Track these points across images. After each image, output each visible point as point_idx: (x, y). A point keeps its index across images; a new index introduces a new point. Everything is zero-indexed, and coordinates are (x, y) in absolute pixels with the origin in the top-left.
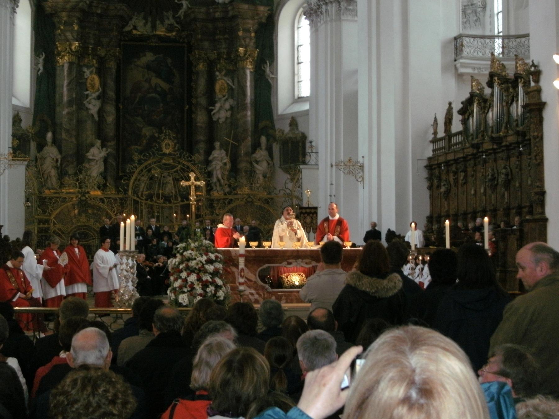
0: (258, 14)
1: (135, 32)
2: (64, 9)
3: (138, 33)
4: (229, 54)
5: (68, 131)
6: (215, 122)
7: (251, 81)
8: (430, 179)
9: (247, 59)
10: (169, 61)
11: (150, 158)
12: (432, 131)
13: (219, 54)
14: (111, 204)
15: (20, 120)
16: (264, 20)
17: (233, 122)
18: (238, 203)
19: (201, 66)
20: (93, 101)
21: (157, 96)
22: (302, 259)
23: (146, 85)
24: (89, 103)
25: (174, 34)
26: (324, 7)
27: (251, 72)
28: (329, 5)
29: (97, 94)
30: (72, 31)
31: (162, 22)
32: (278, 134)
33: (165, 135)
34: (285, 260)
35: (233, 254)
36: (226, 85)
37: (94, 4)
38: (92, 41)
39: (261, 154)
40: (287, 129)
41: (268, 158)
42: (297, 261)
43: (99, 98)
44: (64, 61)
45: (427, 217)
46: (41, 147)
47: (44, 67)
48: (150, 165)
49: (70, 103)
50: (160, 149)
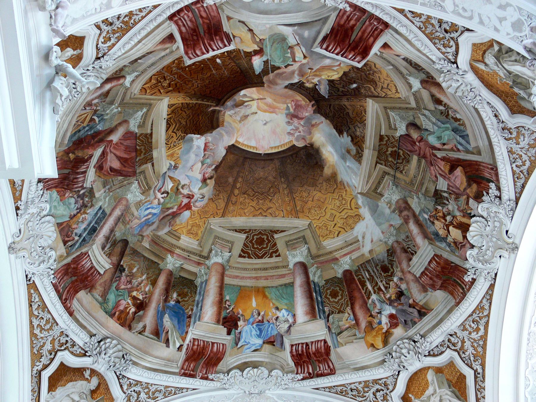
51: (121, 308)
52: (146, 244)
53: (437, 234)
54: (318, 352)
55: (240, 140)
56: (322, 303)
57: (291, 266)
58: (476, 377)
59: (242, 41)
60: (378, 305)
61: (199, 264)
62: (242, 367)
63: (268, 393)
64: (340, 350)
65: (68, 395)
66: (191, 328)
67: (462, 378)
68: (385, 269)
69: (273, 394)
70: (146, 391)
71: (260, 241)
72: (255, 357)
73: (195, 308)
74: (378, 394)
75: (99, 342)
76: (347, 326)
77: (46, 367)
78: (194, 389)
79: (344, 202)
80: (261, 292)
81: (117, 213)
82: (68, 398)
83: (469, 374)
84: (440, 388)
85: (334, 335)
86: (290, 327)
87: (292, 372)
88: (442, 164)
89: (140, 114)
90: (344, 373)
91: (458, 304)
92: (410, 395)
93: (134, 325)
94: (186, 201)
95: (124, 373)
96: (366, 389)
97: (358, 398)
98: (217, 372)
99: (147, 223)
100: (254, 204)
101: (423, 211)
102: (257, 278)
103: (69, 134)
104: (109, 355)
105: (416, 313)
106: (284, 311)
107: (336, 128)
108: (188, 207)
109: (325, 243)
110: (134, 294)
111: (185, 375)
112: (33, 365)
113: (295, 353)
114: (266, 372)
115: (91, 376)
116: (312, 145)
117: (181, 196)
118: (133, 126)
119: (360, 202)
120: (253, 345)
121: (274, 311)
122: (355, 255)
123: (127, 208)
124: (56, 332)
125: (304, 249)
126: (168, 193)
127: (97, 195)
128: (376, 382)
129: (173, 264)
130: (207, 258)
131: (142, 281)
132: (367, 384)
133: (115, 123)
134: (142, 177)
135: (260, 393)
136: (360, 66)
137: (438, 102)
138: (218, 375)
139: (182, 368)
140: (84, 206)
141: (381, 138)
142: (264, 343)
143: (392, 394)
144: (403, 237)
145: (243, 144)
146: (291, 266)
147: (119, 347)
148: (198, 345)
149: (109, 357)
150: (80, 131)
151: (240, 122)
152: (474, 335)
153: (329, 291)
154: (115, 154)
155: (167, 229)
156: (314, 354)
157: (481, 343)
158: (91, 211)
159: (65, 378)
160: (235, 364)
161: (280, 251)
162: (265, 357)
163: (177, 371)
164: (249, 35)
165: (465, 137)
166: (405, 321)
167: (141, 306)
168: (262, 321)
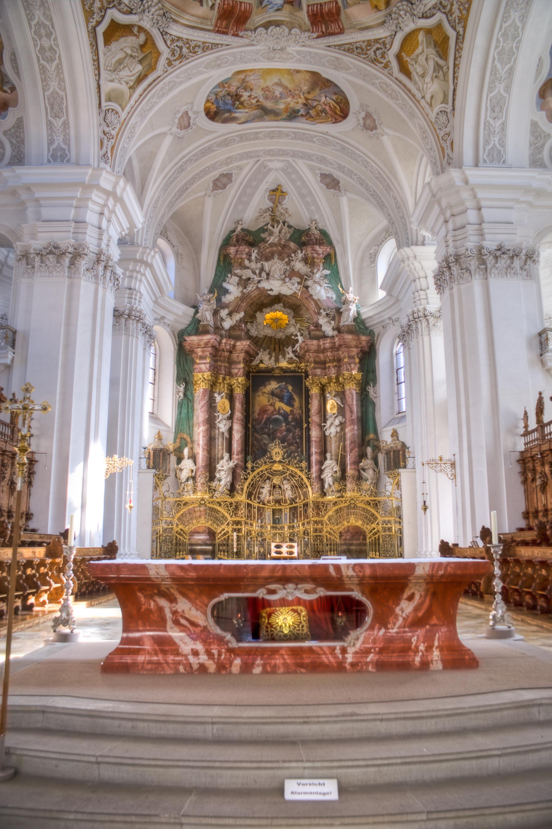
1: (261, 365)
7: (357, 401)
8: (524, 473)
10: (290, 388)
12: (522, 424)
13: (330, 379)
14: (227, 507)
18: (342, 505)
21: (280, 417)
22: (297, 584)
23: (271, 409)
25: (294, 365)
27: (357, 393)
31: (284, 357)
32: (382, 445)
33: (276, 445)
34: (263, 586)
36: (335, 404)
38: (223, 372)
39: (367, 463)
41: (373, 466)
42: (286, 586)
48: (262, 471)
50: (271, 458)
54: (330, 12)
58: (457, 39)
62: (267, 25)
63: (289, 50)
65: (122, 49)
67: (446, 39)
69: (293, 51)
70: (187, 46)
72: (277, 16)
74: (378, 52)
77: (99, 23)
78: (227, 45)
82: (121, 52)
83: (452, 34)
84: (427, 48)
87: (308, 31)
90: (352, 33)
92: (403, 54)
95: (166, 30)
96: (369, 48)
97: (361, 56)
98: (246, 30)
104: (151, 13)
111: (219, 32)
112: (88, 22)
113: (310, 13)
114: (287, 30)
115: (138, 32)
120: (276, 5)
128: (376, 41)
132: (369, 43)
135: (282, 50)
138: (247, 33)
139: (216, 26)
143: (389, 52)
147: (160, 5)
148: (228, 4)
149: (153, 15)
156: (327, 14)
157: (467, 6)
159: (117, 34)
160: (261, 23)
162: (286, 17)
163: (212, 28)
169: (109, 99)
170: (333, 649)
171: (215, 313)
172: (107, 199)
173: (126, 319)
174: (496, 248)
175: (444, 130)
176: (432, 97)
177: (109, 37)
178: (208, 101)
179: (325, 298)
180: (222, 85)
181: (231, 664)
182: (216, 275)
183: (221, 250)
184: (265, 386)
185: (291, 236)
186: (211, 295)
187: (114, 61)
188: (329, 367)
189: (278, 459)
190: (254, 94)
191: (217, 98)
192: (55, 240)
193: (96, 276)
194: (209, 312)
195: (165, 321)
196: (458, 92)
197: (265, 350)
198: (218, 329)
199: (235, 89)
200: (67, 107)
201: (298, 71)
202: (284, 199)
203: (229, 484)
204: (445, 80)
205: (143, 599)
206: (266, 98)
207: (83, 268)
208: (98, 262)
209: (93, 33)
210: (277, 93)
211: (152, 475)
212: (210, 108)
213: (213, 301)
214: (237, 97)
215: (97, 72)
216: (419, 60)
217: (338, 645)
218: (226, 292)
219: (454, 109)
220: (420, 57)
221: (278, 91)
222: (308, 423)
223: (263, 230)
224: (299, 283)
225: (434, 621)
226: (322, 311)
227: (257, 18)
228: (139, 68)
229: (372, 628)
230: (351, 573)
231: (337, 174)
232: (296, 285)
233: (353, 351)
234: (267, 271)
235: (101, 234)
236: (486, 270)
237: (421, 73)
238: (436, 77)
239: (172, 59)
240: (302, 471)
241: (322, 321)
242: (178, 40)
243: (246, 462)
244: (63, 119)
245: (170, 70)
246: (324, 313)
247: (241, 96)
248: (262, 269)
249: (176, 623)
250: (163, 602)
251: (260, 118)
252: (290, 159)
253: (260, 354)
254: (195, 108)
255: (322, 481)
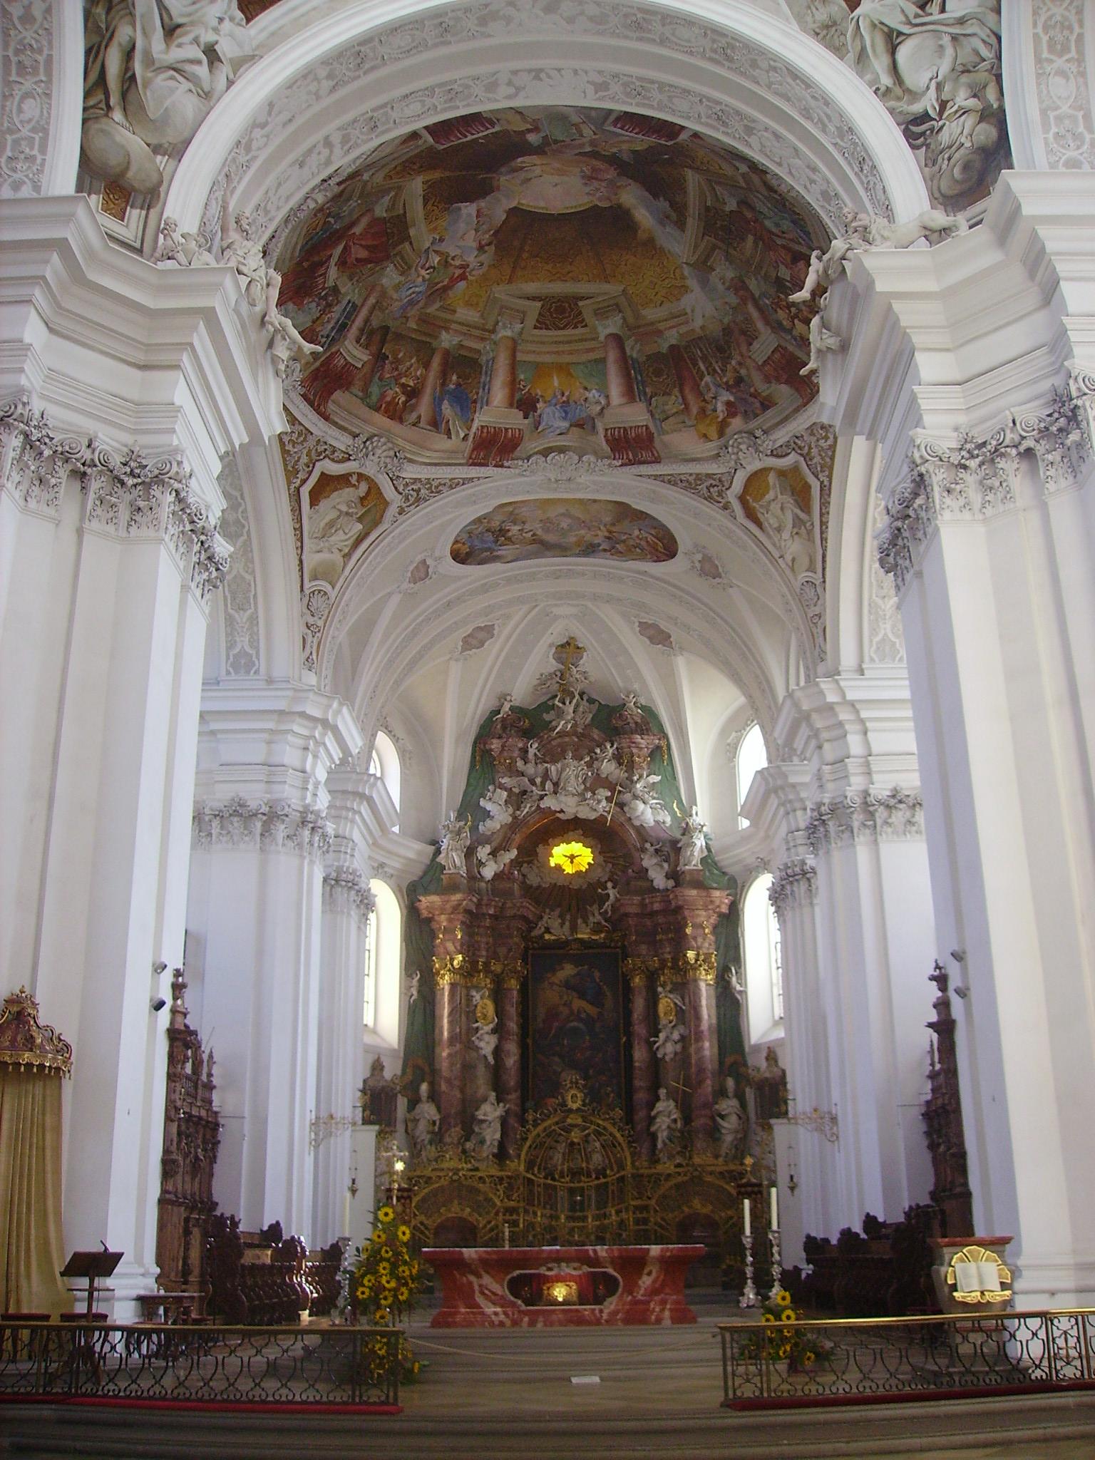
0: (712, 902)
1: (547, 937)
2: (442, 912)
3: (553, 938)
4: (675, 960)
5: (449, 1081)
6: (661, 1059)
8: (928, 1134)
9: (700, 966)
10: (597, 974)
11: (549, 1117)
13: (663, 963)
15: (382, 1068)
16: (724, 909)
17: (683, 1057)
19: (637, 980)
20: (487, 1037)
21: (581, 1025)
24: (480, 1039)
25: (602, 935)
26: (788, 887)
28: (796, 884)
29: (491, 1026)
30: (454, 941)
31: (586, 922)
34: (541, 1265)
35: (466, 1256)
36: (672, 1005)
37: (484, 902)
38: (484, 953)
39: (728, 1105)
40: (763, 1064)
43: (494, 1031)
44: (445, 981)
45: (931, 1193)
46: (414, 1103)
47: (419, 992)
49: (453, 1040)
50: (564, 1104)
51: (388, 399)
52: (412, 325)
53: (780, 324)
55: (523, 202)
56: (643, 383)
57: (602, 338)
59: (508, 122)
60: (713, 389)
61: (483, 339)
62: (545, 453)
64: (666, 438)
66: (477, 414)
67: (807, 487)
68: (720, 349)
71: (561, 310)
72: (559, 441)
73: (481, 391)
74: (712, 490)
75: (365, 443)
76: (675, 410)
77: (304, 482)
79: (666, 270)
80: (564, 369)
81: (372, 300)
84: (782, 494)
85: (658, 422)
86: (603, 409)
87: (608, 458)
88: (783, 252)
89: (387, 198)
91: (805, 405)
93: (406, 416)
94: (458, 272)
98: (512, 459)
99: (412, 303)
100: (549, 267)
101: (764, 295)
102: (557, 353)
103: (299, 247)
105: (758, 405)
106: (594, 391)
107: (649, 190)
108: (463, 277)
109: (644, 312)
110: (403, 380)
112: (289, 483)
114: (576, 458)
116: (620, 206)
117: (452, 268)
118: (380, 211)
119: (686, 273)
121: (582, 391)
122: (683, 329)
123: (384, 294)
124: (311, 443)
125: (618, 319)
126: (434, 268)
127: (343, 291)
128: (709, 476)
129: (450, 341)
130: (493, 331)
131: (411, 366)
132: (698, 477)
133: (355, 217)
134: (398, 258)
136: (669, 144)
137: (771, 189)
139: (470, 458)
140: (329, 305)
141: (707, 209)
142: (571, 426)
143: (728, 492)
144: (740, 318)
145: (528, 206)
146: (602, 338)
150: (312, 238)
151: (521, 184)
152: (822, 442)
153: (651, 369)
154: (361, 245)
155: (437, 305)
157: (830, 453)
158: (338, 309)
161: (587, 321)
164: (518, 117)
165: (808, 234)
166: (746, 411)
167: (413, 394)
168: (568, 402)
169: (315, 578)
170: (594, 1310)
171: (470, 853)
172: (315, 728)
173: (332, 887)
174: (889, 793)
175: (813, 608)
176: (793, 560)
177: (315, 497)
178: (456, 542)
179: (652, 823)
180: (478, 521)
181: (522, 1320)
182: (468, 784)
183: (475, 743)
184: (554, 971)
185: (592, 719)
186: (462, 823)
187: (322, 525)
188: (661, 940)
189: (575, 1106)
190: (527, 527)
191: (470, 537)
192: (241, 795)
193: (300, 845)
194: (459, 852)
195: (386, 869)
196: (828, 559)
197: (553, 911)
198: (474, 877)
199: (498, 523)
200: (255, 596)
201: (595, 501)
202: (581, 658)
203: (496, 1143)
204: (810, 539)
205: (458, 1276)
206: (547, 531)
207: (282, 835)
208: (303, 823)
209: (296, 497)
210: (564, 525)
211: (374, 1134)
212: (459, 549)
213: (466, 834)
214: (502, 532)
215: (299, 544)
216: (771, 508)
217: (597, 1307)
218: (487, 815)
219: (824, 582)
220: (773, 505)
221: (565, 524)
222: (629, 1034)
223: (546, 707)
224: (609, 800)
225: (667, 1290)
226: (648, 845)
227: (530, 445)
228: (360, 527)
229: (622, 1294)
230: (604, 1254)
231: (664, 625)
232: (604, 803)
233: (698, 915)
234: (555, 779)
235: (306, 781)
236: (875, 827)
237: (776, 525)
238: (797, 533)
239: (404, 505)
240: (614, 1124)
241: (648, 861)
242: (413, 483)
243: (524, 1111)
244: (249, 612)
245: (401, 518)
246: (652, 849)
247: (509, 530)
248: (546, 776)
249: (482, 1293)
250: (472, 1278)
251: (536, 555)
252: (589, 604)
253: (546, 917)
254: (437, 554)
255: (653, 1137)
